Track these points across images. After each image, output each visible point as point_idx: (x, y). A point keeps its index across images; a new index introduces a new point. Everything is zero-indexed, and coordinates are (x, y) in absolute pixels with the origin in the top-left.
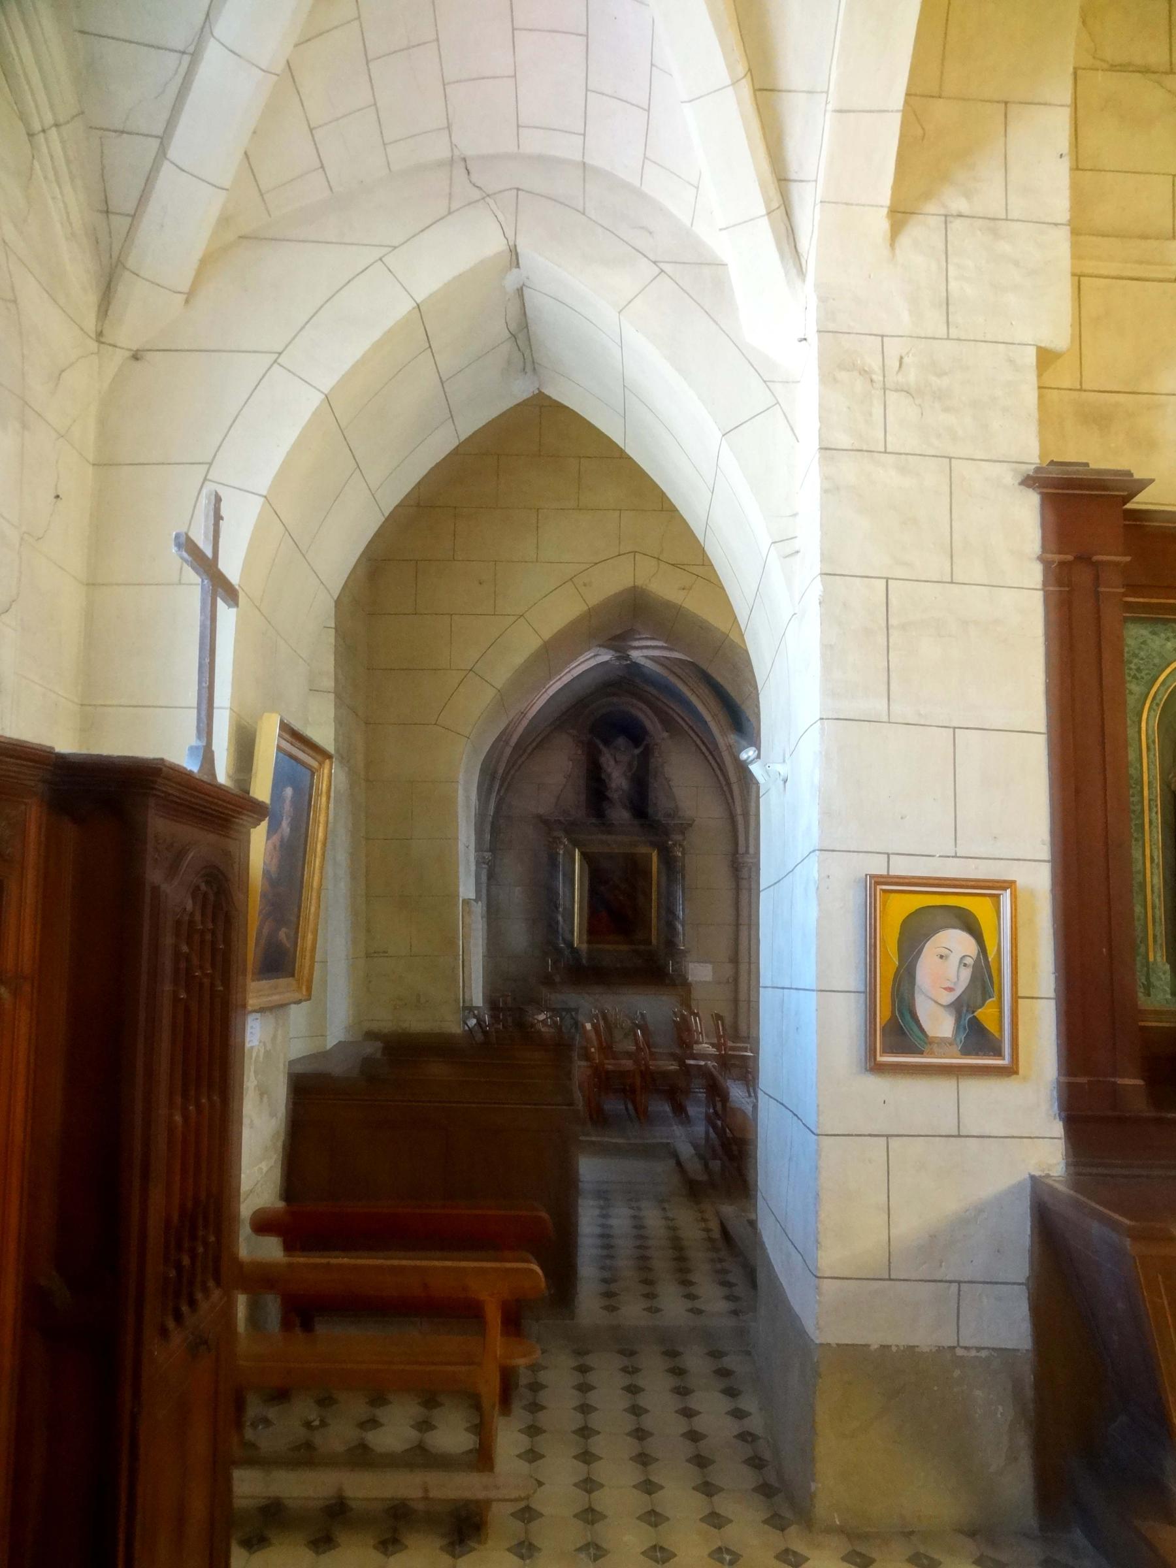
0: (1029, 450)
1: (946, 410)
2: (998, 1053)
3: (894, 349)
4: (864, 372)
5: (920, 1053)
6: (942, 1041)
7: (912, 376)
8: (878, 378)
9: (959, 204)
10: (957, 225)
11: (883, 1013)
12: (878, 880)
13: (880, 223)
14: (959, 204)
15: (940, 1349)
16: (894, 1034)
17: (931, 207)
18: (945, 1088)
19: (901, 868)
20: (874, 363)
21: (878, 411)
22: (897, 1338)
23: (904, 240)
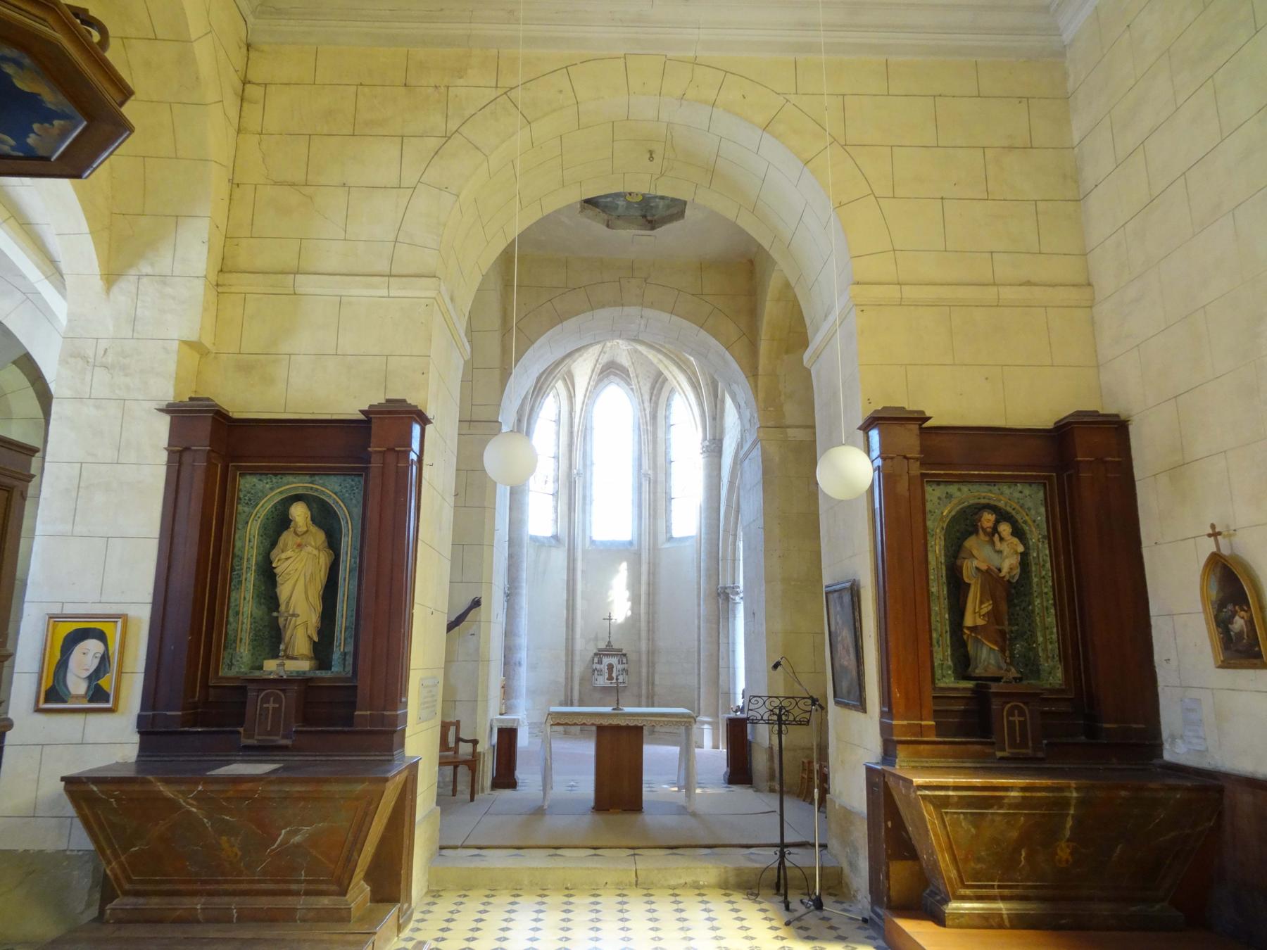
0: (167, 392)
1: (126, 375)
2: (107, 701)
3: (103, 344)
4: (85, 358)
5: (64, 701)
6: (77, 697)
7: (110, 359)
8: (91, 360)
9: (146, 269)
10: (145, 280)
11: (47, 683)
12: (51, 617)
13: (98, 283)
14: (146, 269)
15: (58, 852)
16: (53, 696)
17: (133, 272)
18: (79, 718)
19: (69, 610)
20: (90, 353)
21: (88, 378)
22: (34, 846)
23: (115, 289)
